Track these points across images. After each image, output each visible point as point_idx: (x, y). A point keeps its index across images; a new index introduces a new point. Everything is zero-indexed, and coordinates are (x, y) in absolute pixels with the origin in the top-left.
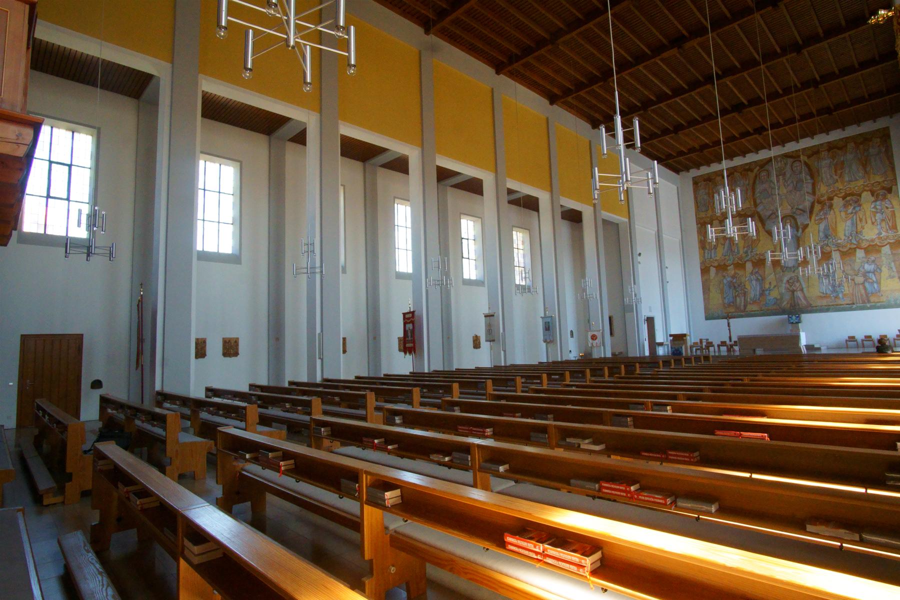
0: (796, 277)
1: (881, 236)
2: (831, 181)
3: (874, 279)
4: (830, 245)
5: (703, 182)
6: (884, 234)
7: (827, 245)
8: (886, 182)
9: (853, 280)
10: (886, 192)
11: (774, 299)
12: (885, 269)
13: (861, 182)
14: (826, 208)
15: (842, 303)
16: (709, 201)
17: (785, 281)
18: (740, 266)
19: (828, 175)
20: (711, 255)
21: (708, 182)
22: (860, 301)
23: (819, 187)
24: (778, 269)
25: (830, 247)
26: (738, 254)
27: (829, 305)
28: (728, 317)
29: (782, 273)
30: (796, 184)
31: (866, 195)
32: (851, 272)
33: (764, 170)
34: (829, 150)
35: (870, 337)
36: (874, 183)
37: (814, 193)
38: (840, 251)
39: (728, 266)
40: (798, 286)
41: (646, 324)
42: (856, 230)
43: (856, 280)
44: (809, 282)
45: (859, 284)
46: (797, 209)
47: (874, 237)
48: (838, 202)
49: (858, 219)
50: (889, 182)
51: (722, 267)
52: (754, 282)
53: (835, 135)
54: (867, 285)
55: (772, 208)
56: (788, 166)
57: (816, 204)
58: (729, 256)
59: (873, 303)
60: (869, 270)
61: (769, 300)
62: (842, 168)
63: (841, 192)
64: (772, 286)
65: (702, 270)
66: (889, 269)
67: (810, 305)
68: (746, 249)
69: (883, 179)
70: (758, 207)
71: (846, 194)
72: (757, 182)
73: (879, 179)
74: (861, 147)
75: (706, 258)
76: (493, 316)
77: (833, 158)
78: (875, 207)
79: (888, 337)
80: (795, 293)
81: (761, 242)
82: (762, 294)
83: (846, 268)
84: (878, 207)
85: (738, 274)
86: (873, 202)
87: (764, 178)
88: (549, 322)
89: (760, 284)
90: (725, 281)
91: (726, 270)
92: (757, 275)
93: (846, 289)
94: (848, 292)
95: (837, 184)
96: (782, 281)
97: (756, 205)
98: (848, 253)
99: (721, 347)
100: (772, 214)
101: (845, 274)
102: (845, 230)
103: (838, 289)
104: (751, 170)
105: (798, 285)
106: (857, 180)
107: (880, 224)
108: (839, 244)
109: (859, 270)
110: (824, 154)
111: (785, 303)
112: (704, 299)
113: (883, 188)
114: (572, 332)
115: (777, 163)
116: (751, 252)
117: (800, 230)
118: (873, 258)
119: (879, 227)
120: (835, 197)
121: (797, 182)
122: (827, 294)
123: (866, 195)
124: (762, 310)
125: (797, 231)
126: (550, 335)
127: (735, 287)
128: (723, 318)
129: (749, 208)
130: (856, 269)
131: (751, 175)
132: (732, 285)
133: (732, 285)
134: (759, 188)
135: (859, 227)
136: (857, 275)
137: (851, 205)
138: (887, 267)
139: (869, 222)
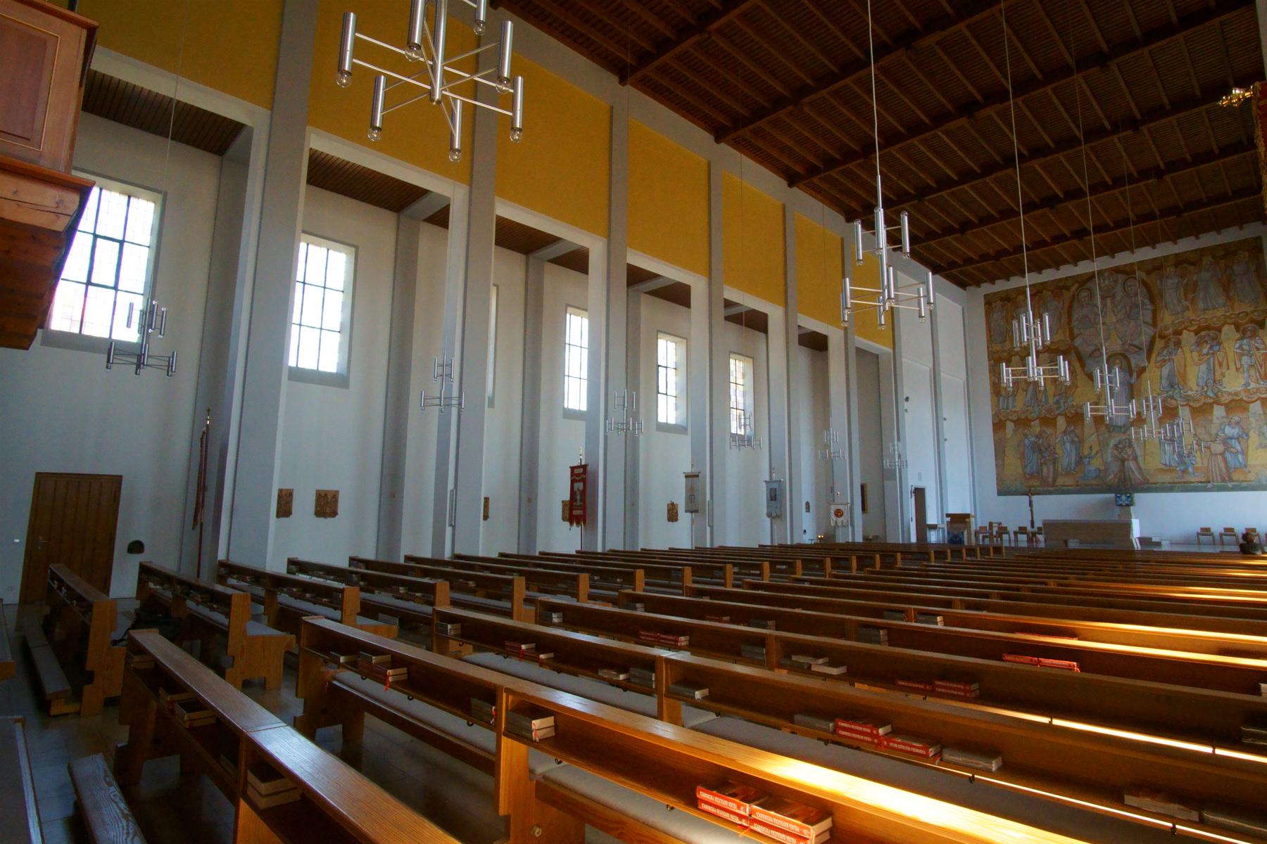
0: (1127, 441)
1: (1250, 388)
2: (1179, 309)
3: (1239, 448)
4: (1176, 397)
6: (1253, 385)
7: (1172, 397)
8: (1256, 314)
9: (1209, 448)
10: (1257, 327)
12: (1253, 435)
14: (1172, 346)
15: (1192, 480)
16: (1007, 329)
17: (1111, 446)
18: (1049, 421)
20: (1007, 406)
21: (1006, 302)
23: (1161, 315)
24: (1103, 429)
25: (1175, 400)
27: (1174, 483)
28: (1029, 493)
30: (1130, 312)
31: (1228, 330)
34: (1177, 265)
35: (1231, 530)
36: (1240, 313)
37: (1154, 324)
38: (1190, 406)
39: (1031, 421)
40: (1129, 453)
41: (913, 498)
43: (1212, 449)
44: (1147, 447)
45: (1216, 455)
48: (1188, 337)
49: (1216, 362)
51: (1022, 422)
52: (1068, 446)
53: (1185, 245)
54: (1228, 455)
56: (1119, 288)
58: (1034, 407)
59: (1236, 481)
61: (1090, 471)
63: (1192, 324)
64: (1094, 452)
65: (994, 424)
66: (1259, 435)
67: (1148, 482)
68: (1057, 398)
69: (1252, 309)
70: (1075, 340)
71: (1199, 327)
72: (1075, 305)
73: (1248, 308)
74: (1222, 262)
75: (1001, 407)
76: (697, 476)
77: (1182, 276)
78: (1240, 347)
79: (1257, 530)
80: (1126, 463)
81: (1078, 390)
82: (1080, 460)
83: (1199, 430)
84: (1245, 347)
85: (1046, 433)
86: (1238, 339)
87: (1085, 300)
88: (775, 489)
91: (1030, 426)
92: (1072, 436)
93: (1199, 460)
94: (1201, 465)
96: (1107, 444)
97: (1073, 337)
98: (1201, 410)
99: (1019, 536)
100: (1093, 352)
101: (1197, 438)
103: (1187, 460)
104: (1068, 289)
105: (1129, 451)
107: (1248, 371)
108: (1189, 396)
109: (1217, 434)
110: (1170, 270)
112: (996, 465)
113: (1252, 321)
114: (807, 504)
115: (1104, 280)
117: (1135, 374)
118: (1237, 419)
119: (1246, 375)
120: (1185, 331)
121: (1131, 307)
122: (1171, 466)
123: (1228, 330)
124: (1078, 486)
125: (1131, 375)
126: (776, 507)
127: (1040, 451)
128: (1022, 495)
130: (1214, 432)
131: (1067, 295)
132: (1038, 449)
133: (1038, 449)
134: (1078, 313)
135: (1218, 374)
136: (1214, 441)
137: (1206, 342)
138: (1257, 432)
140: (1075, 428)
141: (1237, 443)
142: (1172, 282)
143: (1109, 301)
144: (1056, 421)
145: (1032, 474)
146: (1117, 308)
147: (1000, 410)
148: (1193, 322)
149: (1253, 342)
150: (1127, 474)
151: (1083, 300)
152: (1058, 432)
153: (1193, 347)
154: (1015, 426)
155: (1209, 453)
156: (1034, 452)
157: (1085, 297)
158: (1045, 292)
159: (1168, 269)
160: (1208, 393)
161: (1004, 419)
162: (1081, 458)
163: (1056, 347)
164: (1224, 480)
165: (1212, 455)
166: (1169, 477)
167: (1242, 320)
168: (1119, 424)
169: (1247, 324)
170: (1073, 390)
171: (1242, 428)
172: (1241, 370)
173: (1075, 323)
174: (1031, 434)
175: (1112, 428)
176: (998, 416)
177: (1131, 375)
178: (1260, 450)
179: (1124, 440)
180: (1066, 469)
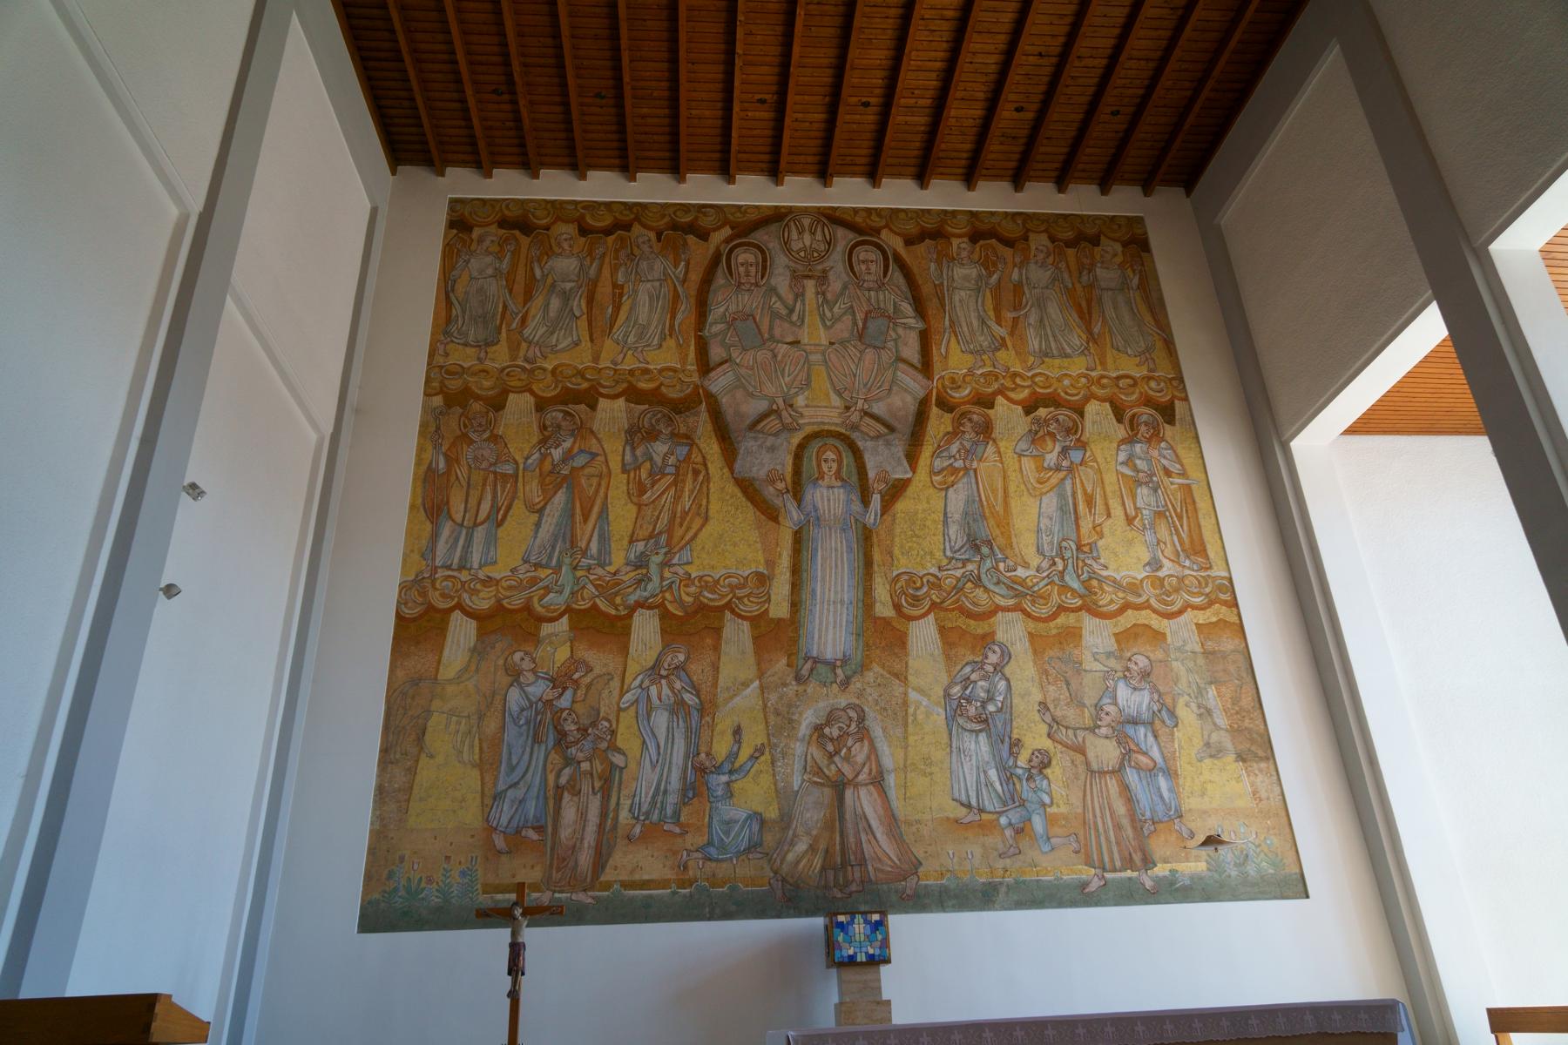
0: (853, 714)
1: (1160, 574)
3: (1155, 753)
4: (986, 583)
5: (493, 229)
8: (1153, 384)
9: (1083, 752)
10: (1160, 418)
11: (749, 817)
12: (1187, 714)
13: (1078, 366)
16: (505, 306)
17: (804, 729)
19: (973, 315)
20: (465, 557)
21: (517, 232)
22: (1116, 856)
23: (943, 351)
25: (986, 590)
26: (602, 565)
29: (793, 687)
32: (1070, 714)
33: (749, 244)
34: (975, 237)
36: (1118, 378)
37: (926, 367)
38: (1024, 611)
39: (541, 620)
40: (860, 758)
42: (1074, 536)
43: (1091, 755)
44: (911, 739)
45: (1102, 773)
46: (866, 414)
47: (1140, 577)
48: (1006, 414)
50: (1162, 384)
52: (661, 720)
54: (1132, 776)
55: (770, 390)
56: (837, 260)
57: (935, 410)
60: (1133, 711)
61: (729, 823)
62: (1017, 307)
65: (400, 617)
66: (1200, 715)
68: (640, 546)
70: (712, 374)
71: (1034, 393)
72: (720, 280)
73: (1130, 367)
74: (1071, 252)
75: (438, 562)
77: (988, 264)
78: (1129, 462)
80: (849, 793)
85: (590, 669)
86: (1123, 442)
89: (688, 729)
90: (514, 695)
91: (533, 637)
94: (1063, 809)
95: (1001, 354)
96: (791, 724)
97: (705, 367)
100: (763, 416)
101: (1048, 718)
102: (1039, 531)
103: (1025, 789)
104: (704, 236)
105: (860, 753)
106: (1067, 356)
107: (1153, 526)
108: (1022, 582)
109: (1098, 707)
110: (959, 245)
111: (801, 847)
112: (381, 791)
113: (1148, 402)
116: (665, 564)
117: (876, 499)
118: (1142, 662)
120: (1000, 400)
122: (981, 811)
124: (682, 884)
125: (865, 502)
127: (562, 735)
129: (675, 370)
130: (1089, 701)
131: (699, 252)
134: (723, 304)
135: (1086, 525)
136: (1092, 729)
137: (1052, 435)
138: (1194, 706)
139: (1117, 511)
140: (688, 658)
141: (1150, 735)
142: (964, 273)
143: (810, 285)
144: (629, 627)
145: (518, 831)
146: (831, 310)
147: (435, 570)
148: (1018, 380)
149: (1155, 453)
150: (852, 839)
151: (742, 269)
152: (633, 668)
153: (1023, 445)
154: (482, 633)
155: (1082, 768)
156: (537, 740)
157: (746, 264)
158: (637, 229)
159: (955, 242)
160: (1067, 578)
161: (442, 605)
162: (701, 770)
163: (651, 386)
164: (1129, 863)
165: (1092, 772)
166: (978, 851)
167: (1126, 395)
168: (829, 655)
169: (1139, 406)
170: (695, 527)
171: (1158, 691)
172: (1136, 522)
173: (714, 328)
174: (534, 671)
175: (809, 665)
176: (424, 594)
177: (865, 502)
178: (1208, 761)
179: (844, 710)
180: (647, 814)
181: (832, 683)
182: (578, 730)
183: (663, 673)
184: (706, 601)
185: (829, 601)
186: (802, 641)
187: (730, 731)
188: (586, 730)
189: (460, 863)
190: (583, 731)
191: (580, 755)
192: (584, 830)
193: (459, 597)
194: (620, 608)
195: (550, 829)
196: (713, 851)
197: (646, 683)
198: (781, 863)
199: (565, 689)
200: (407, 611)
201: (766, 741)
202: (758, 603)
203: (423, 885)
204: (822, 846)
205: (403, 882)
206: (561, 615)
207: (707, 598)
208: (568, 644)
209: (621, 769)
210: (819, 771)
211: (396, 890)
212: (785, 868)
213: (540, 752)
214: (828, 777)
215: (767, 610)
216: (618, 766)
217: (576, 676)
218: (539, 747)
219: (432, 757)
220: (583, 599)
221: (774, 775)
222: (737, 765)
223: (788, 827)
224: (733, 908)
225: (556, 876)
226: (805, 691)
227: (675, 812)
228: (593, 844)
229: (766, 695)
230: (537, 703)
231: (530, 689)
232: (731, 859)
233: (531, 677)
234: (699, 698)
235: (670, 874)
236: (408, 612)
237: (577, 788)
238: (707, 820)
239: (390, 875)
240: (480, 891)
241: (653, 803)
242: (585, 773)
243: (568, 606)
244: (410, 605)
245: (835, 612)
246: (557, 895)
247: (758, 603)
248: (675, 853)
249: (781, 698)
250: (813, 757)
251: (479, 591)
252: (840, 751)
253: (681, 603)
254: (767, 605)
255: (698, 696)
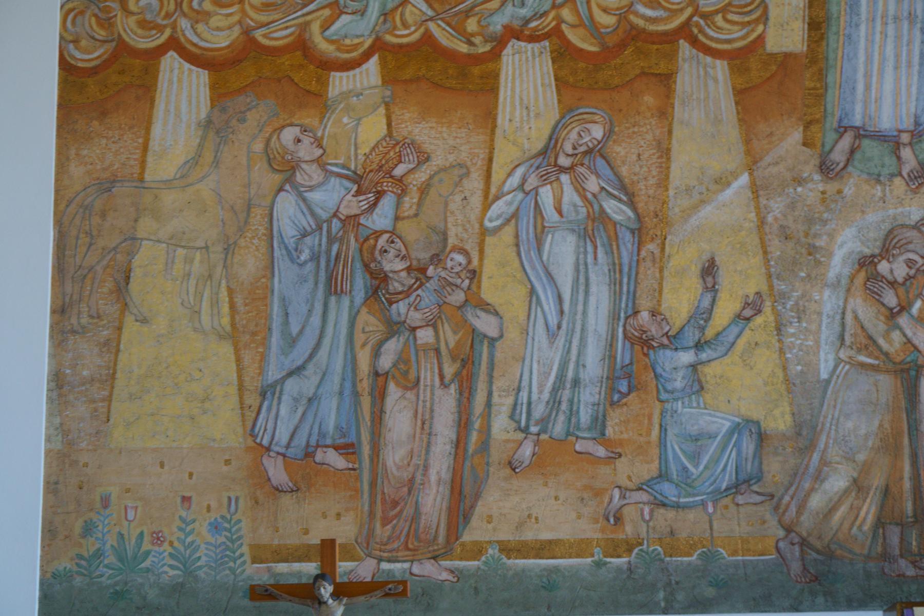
11: (736, 429)
29: (817, 184)
39: (328, 65)
61: (698, 439)
65: (65, 65)
85: (424, 158)
89: (615, 268)
92: (592, 184)
111: (837, 483)
112: (58, 381)
124: (614, 548)
144: (495, 76)
145: (309, 454)
152: (505, 155)
156: (334, 287)
161: (144, 42)
168: (886, 122)
174: (320, 162)
175: (846, 142)
176: (107, 22)
180: (544, 422)
181: (892, 175)
182: (409, 269)
183: (564, 161)
184: (641, 23)
185: (884, 16)
186: (832, 96)
187: (695, 270)
188: (423, 270)
189: (209, 509)
190: (419, 272)
191: (415, 318)
192: (428, 452)
193: (174, 27)
194: (477, 40)
195: (366, 450)
196: (669, 491)
197: (532, 181)
198: (799, 512)
199: (380, 195)
200: (78, 55)
201: (764, 288)
202: (744, 25)
203: (146, 546)
204: (877, 480)
205: (111, 541)
206: (366, 56)
207: (643, 17)
208: (382, 110)
209: (492, 341)
210: (869, 343)
211: (99, 554)
212: (806, 523)
213: (340, 311)
214: (886, 354)
215: (761, 39)
216: (485, 336)
217: (399, 171)
218: (338, 302)
219: (144, 321)
220: (405, 25)
221: (782, 351)
222: (710, 333)
223: (811, 446)
224: (710, 592)
225: (382, 533)
226: (839, 192)
227: (595, 419)
228: (446, 476)
229: (763, 201)
230: (329, 221)
231: (315, 197)
232: (703, 504)
233: (316, 174)
234: (635, 209)
235: (589, 530)
236: (84, 57)
237: (412, 375)
238: (655, 432)
239: (88, 529)
240: (247, 558)
241: (554, 402)
242: (426, 348)
243: (378, 39)
244: (83, 43)
245: (898, 37)
246: (385, 566)
247: (744, 25)
248: (598, 493)
249: (792, 206)
250: (856, 318)
251: (208, 14)
252: (911, 304)
253: (593, 28)
254: (760, 28)
255: (632, 204)
